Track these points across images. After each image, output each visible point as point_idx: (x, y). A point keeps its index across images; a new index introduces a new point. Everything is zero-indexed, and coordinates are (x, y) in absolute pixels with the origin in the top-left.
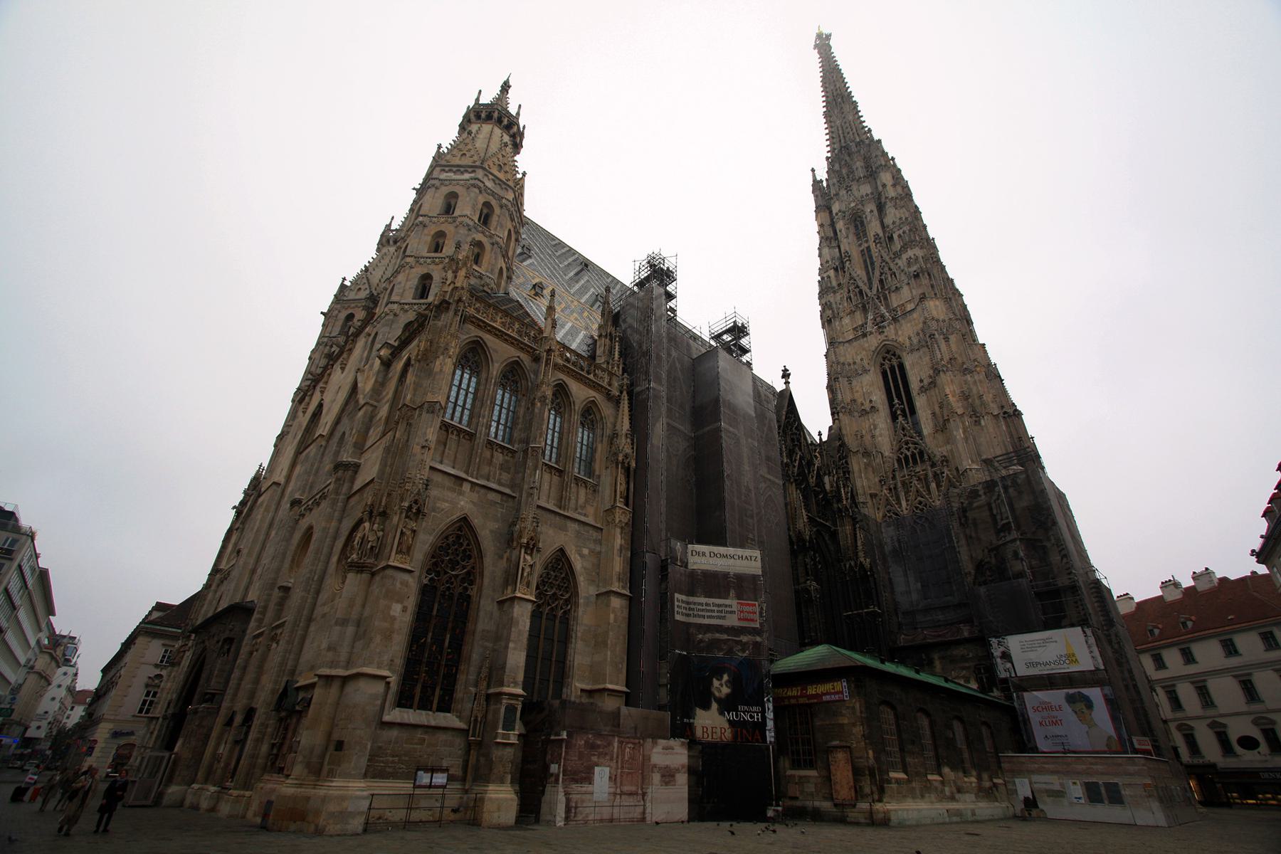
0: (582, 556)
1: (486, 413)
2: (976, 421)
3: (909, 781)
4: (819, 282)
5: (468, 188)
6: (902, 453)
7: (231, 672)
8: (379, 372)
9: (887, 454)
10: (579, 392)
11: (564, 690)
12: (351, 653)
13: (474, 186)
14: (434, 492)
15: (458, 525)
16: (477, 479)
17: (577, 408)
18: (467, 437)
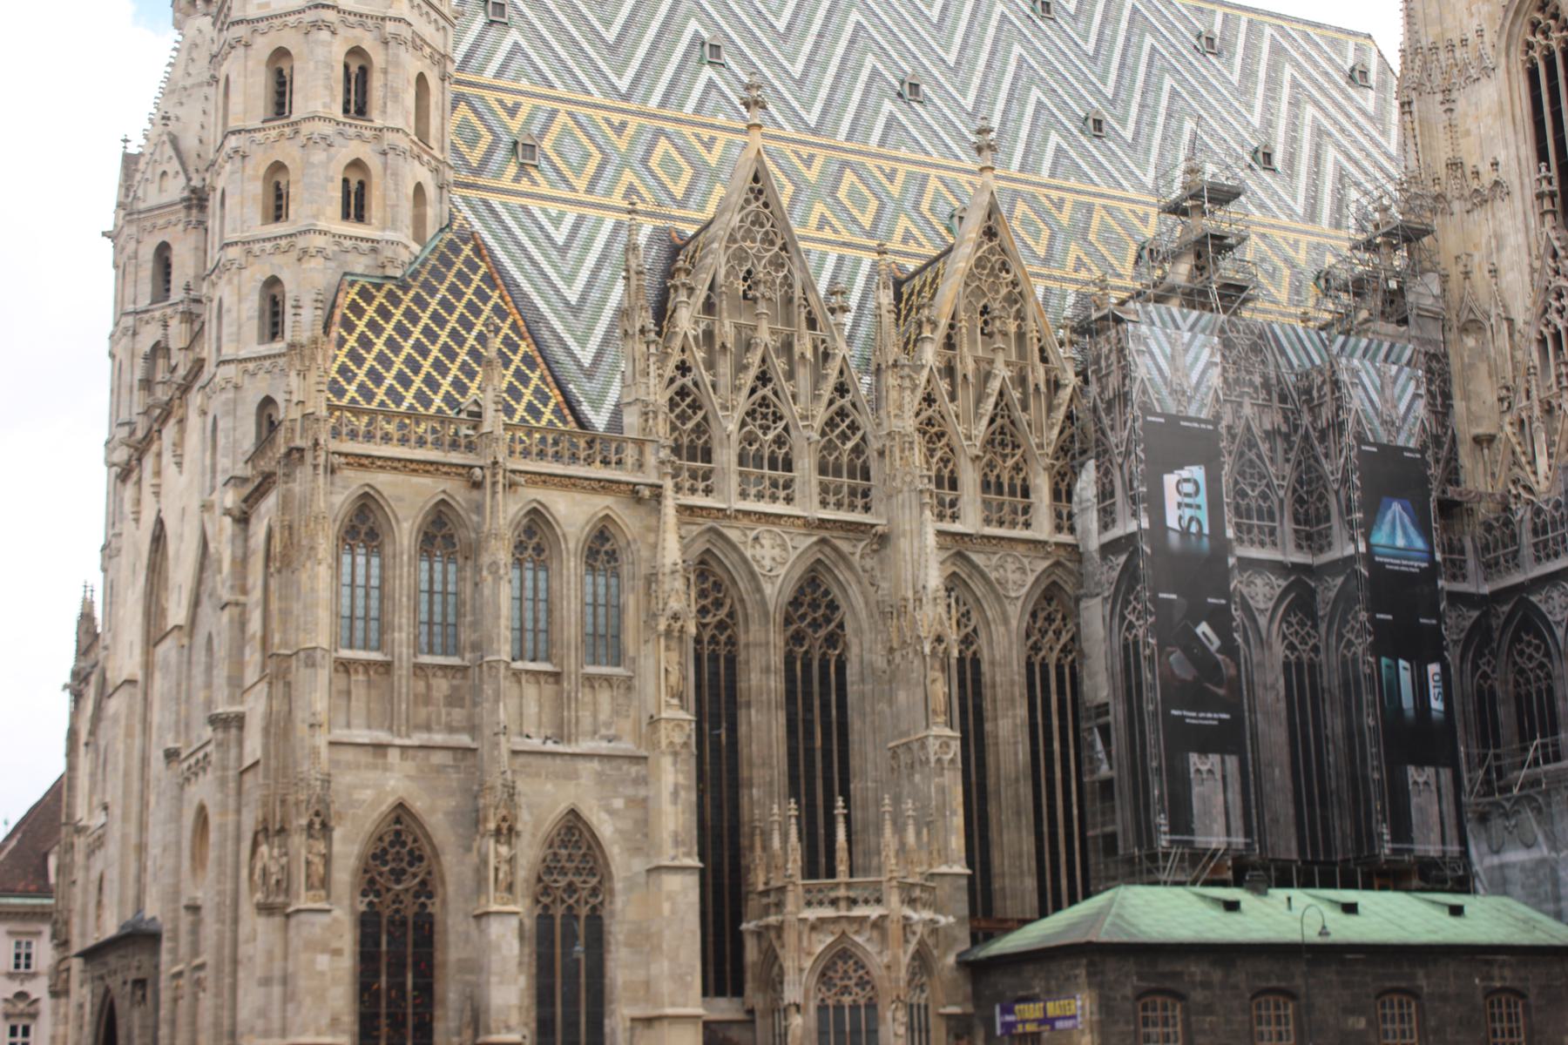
0: (612, 812)
1: (404, 621)
7: (156, 1028)
8: (234, 537)
9: (1519, 324)
11: (607, 1022)
12: (284, 1018)
14: (343, 780)
15: (393, 815)
16: (408, 736)
17: (572, 545)
18: (381, 670)
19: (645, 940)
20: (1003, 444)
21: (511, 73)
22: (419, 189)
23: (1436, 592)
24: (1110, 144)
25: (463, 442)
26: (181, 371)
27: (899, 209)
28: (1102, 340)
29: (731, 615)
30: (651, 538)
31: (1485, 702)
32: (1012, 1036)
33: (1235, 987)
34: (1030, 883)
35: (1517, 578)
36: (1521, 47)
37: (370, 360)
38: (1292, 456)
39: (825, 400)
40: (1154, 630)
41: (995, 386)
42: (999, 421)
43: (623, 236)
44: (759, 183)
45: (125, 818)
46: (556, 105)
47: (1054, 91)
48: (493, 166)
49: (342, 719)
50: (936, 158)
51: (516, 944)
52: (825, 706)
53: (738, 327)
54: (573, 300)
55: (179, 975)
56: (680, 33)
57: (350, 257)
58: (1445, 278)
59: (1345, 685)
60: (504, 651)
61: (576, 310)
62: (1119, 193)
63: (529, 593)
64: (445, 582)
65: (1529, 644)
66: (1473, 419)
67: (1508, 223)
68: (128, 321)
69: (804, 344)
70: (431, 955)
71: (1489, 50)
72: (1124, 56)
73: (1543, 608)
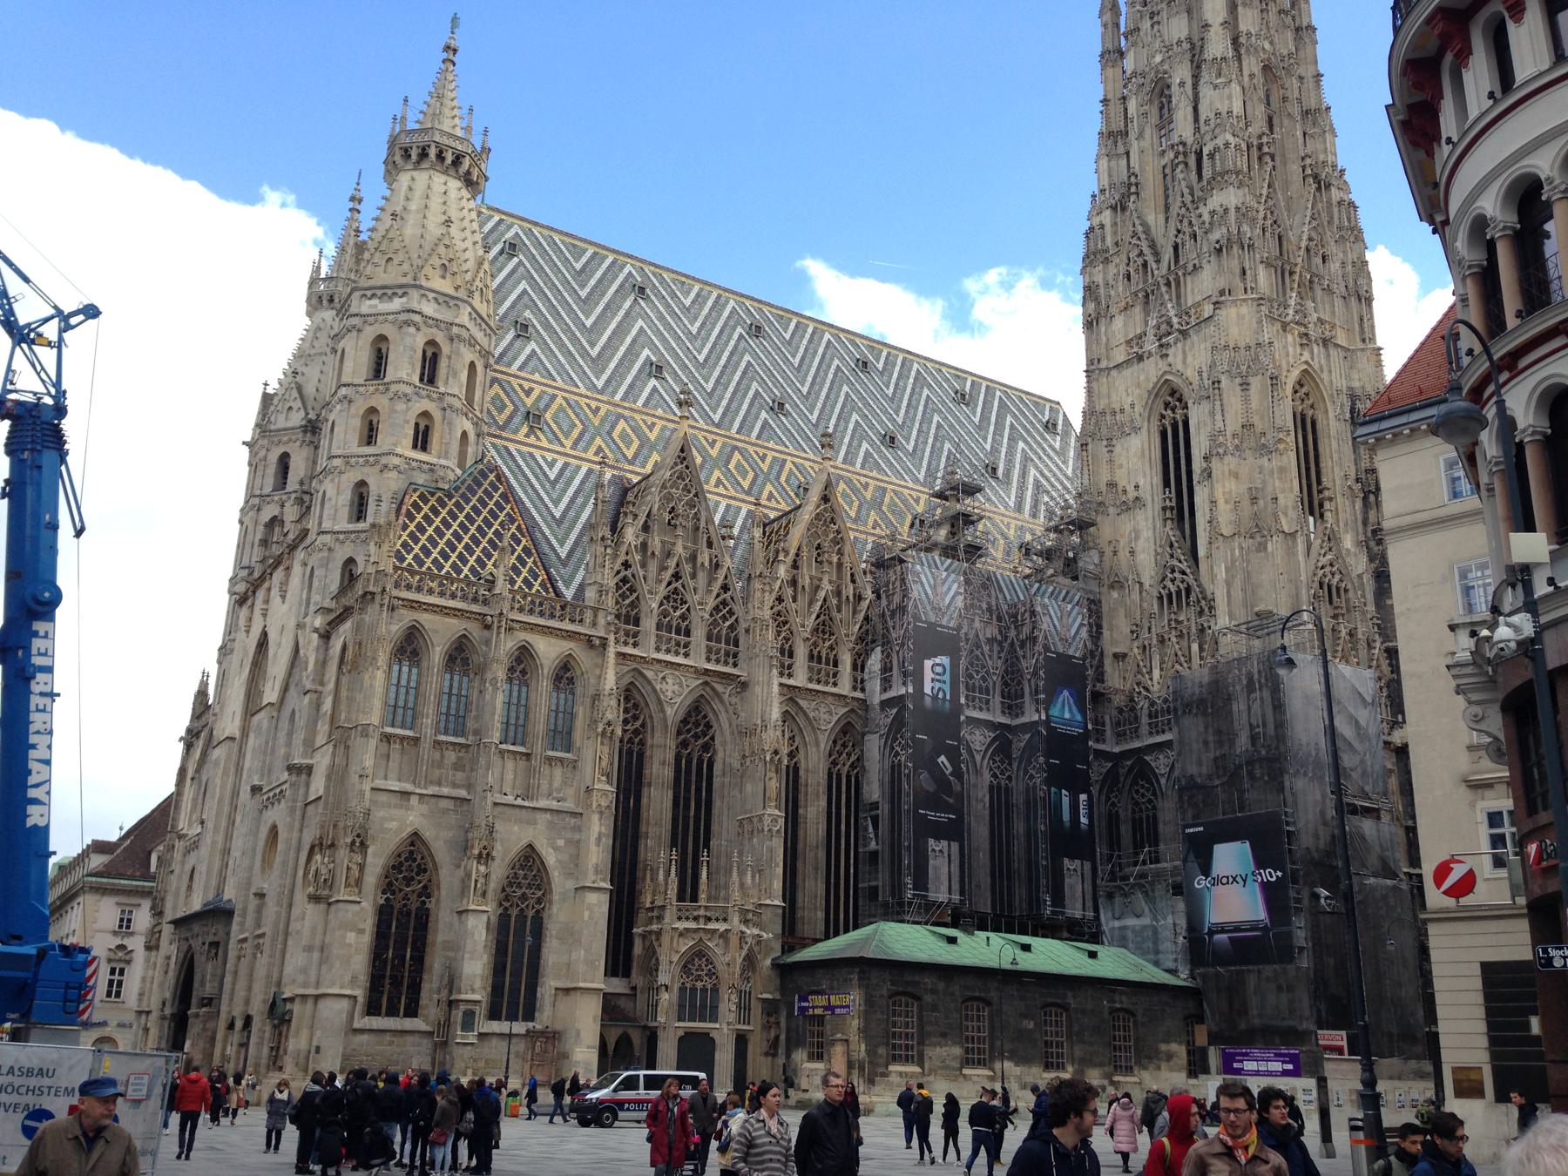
0: (556, 848)
2: (1260, 544)
3: (923, 1074)
4: (1087, 234)
6: (1164, 588)
7: (223, 976)
8: (318, 649)
9: (1146, 586)
10: (548, 650)
12: (319, 975)
13: (408, 323)
14: (379, 814)
16: (426, 788)
19: (571, 936)
20: (824, 632)
22: (464, 434)
23: (1088, 748)
25: (481, 598)
26: (291, 536)
27: (767, 479)
28: (891, 572)
29: (643, 725)
30: (597, 672)
31: (1113, 820)
32: (805, 1016)
33: (953, 994)
34: (821, 915)
35: (1137, 744)
36: (1158, 417)
37: (423, 540)
38: (1002, 655)
39: (715, 593)
40: (910, 758)
41: (822, 594)
42: (822, 617)
43: (593, 479)
44: (683, 454)
45: (216, 829)
46: (556, 392)
48: (512, 426)
49: (382, 774)
50: (791, 450)
51: (484, 932)
52: (698, 790)
53: (663, 542)
54: (558, 515)
55: (245, 940)
56: (638, 356)
57: (415, 473)
58: (1102, 554)
59: (1027, 802)
60: (496, 736)
61: (559, 522)
62: (903, 483)
63: (515, 700)
64: (460, 689)
65: (1143, 787)
66: (1114, 642)
67: (1143, 523)
68: (254, 500)
69: (704, 557)
70: (425, 937)
71: (1138, 417)
72: (910, 400)
73: (1153, 764)
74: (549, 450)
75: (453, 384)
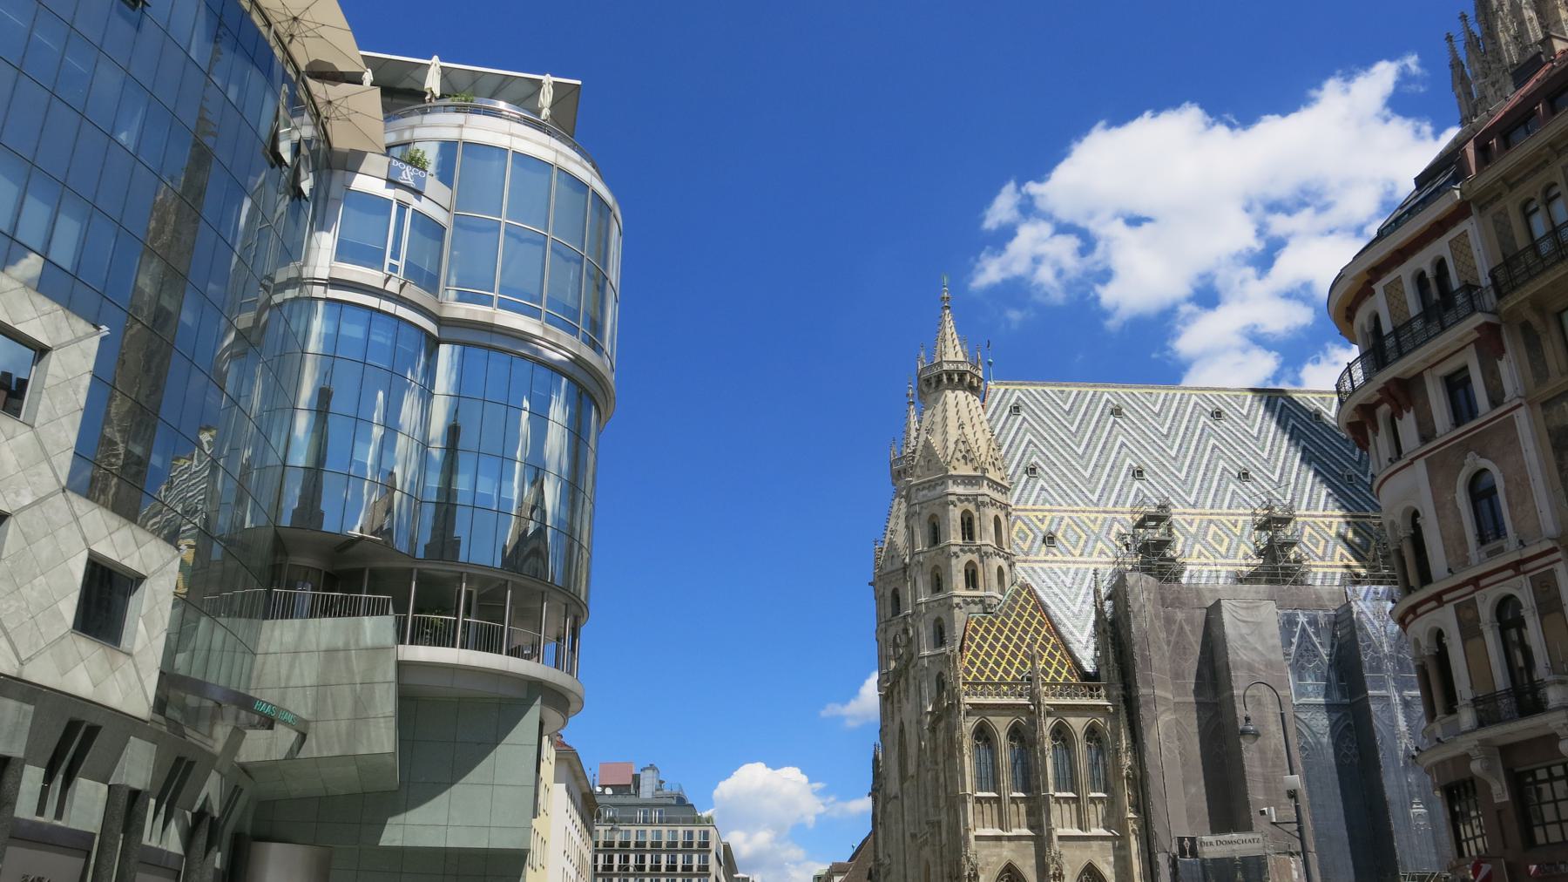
0: (1108, 863)
5: (944, 507)
13: (947, 504)
14: (983, 853)
21: (1041, 501)
22: (1000, 569)
24: (1359, 487)
46: (1062, 514)
47: (1325, 463)
48: (1035, 550)
56: (1122, 465)
74: (1064, 562)
75: (987, 539)
